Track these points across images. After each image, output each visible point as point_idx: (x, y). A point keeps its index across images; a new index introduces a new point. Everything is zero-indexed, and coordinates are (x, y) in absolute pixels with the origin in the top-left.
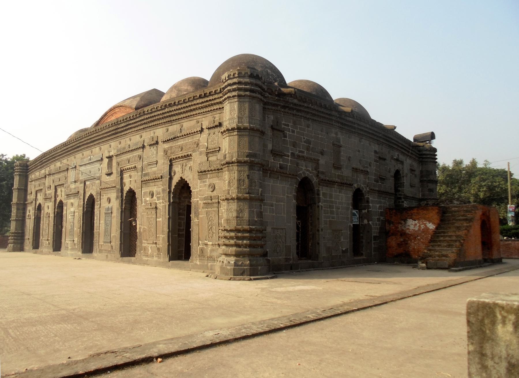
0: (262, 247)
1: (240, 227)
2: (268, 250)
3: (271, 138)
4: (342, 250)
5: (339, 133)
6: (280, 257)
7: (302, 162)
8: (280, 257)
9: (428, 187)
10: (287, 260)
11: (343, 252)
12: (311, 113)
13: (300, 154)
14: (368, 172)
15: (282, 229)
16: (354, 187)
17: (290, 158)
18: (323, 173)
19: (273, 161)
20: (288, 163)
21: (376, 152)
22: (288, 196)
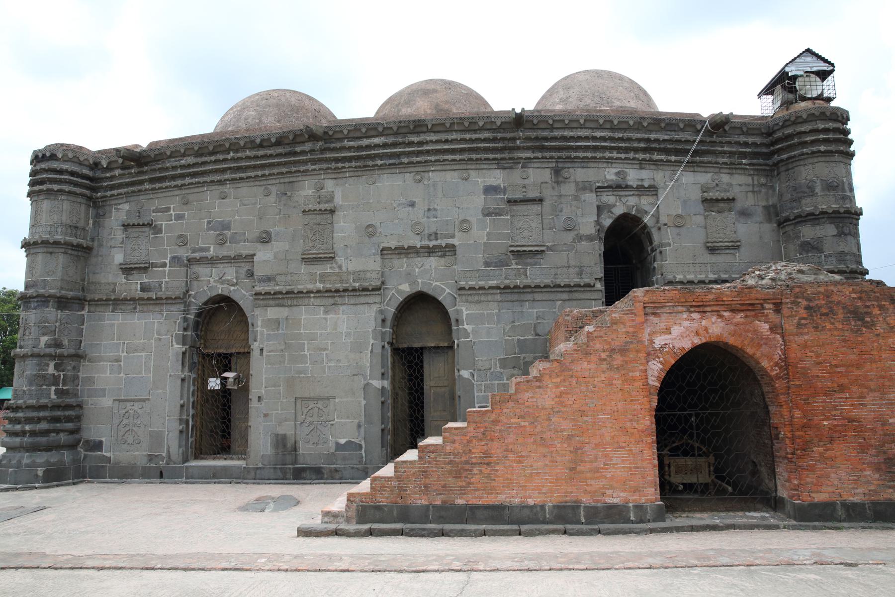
0: (72, 432)
1: (21, 401)
2: (103, 439)
3: (122, 243)
4: (337, 444)
5: (329, 185)
6: (137, 453)
7: (203, 271)
8: (137, 453)
9: (798, 237)
10: (151, 458)
11: (338, 446)
12: (230, 168)
13: (197, 255)
14: (454, 246)
15: (144, 400)
16: (399, 292)
17: (167, 269)
18: (268, 279)
19: (124, 281)
20: (168, 280)
21: (490, 190)
22: (160, 339)
